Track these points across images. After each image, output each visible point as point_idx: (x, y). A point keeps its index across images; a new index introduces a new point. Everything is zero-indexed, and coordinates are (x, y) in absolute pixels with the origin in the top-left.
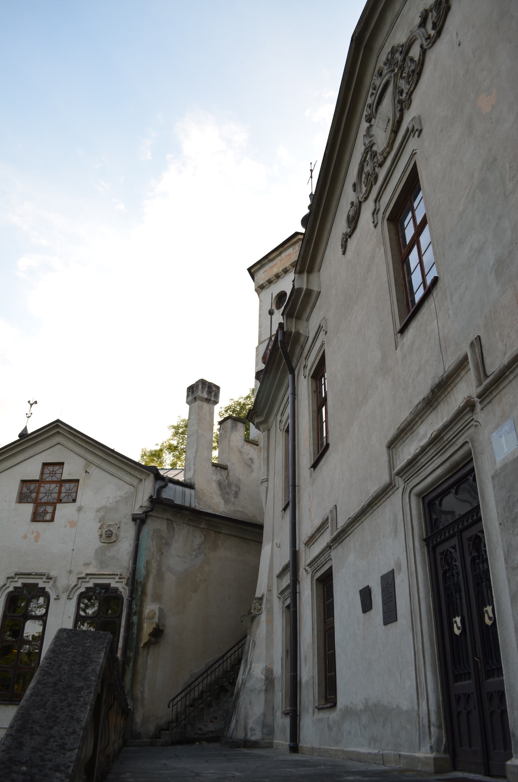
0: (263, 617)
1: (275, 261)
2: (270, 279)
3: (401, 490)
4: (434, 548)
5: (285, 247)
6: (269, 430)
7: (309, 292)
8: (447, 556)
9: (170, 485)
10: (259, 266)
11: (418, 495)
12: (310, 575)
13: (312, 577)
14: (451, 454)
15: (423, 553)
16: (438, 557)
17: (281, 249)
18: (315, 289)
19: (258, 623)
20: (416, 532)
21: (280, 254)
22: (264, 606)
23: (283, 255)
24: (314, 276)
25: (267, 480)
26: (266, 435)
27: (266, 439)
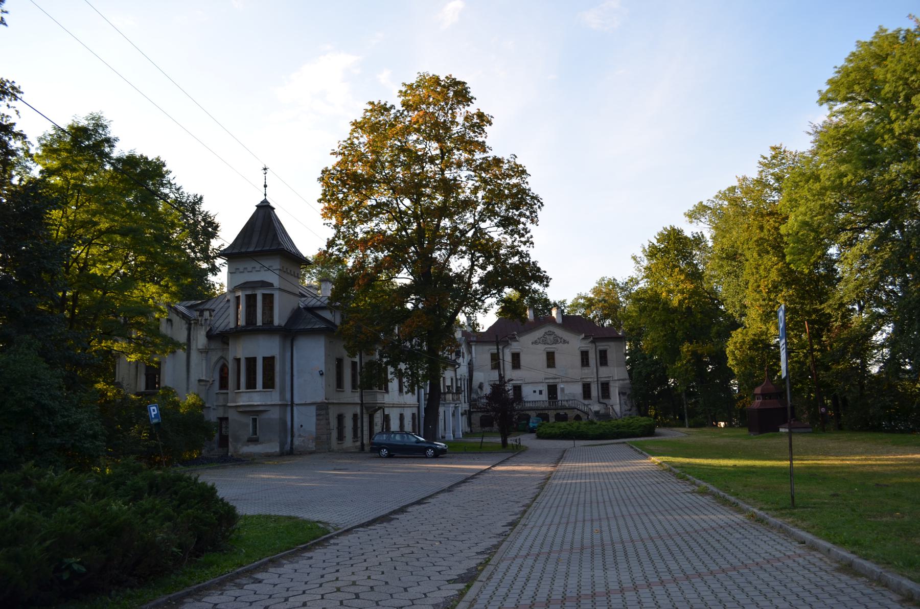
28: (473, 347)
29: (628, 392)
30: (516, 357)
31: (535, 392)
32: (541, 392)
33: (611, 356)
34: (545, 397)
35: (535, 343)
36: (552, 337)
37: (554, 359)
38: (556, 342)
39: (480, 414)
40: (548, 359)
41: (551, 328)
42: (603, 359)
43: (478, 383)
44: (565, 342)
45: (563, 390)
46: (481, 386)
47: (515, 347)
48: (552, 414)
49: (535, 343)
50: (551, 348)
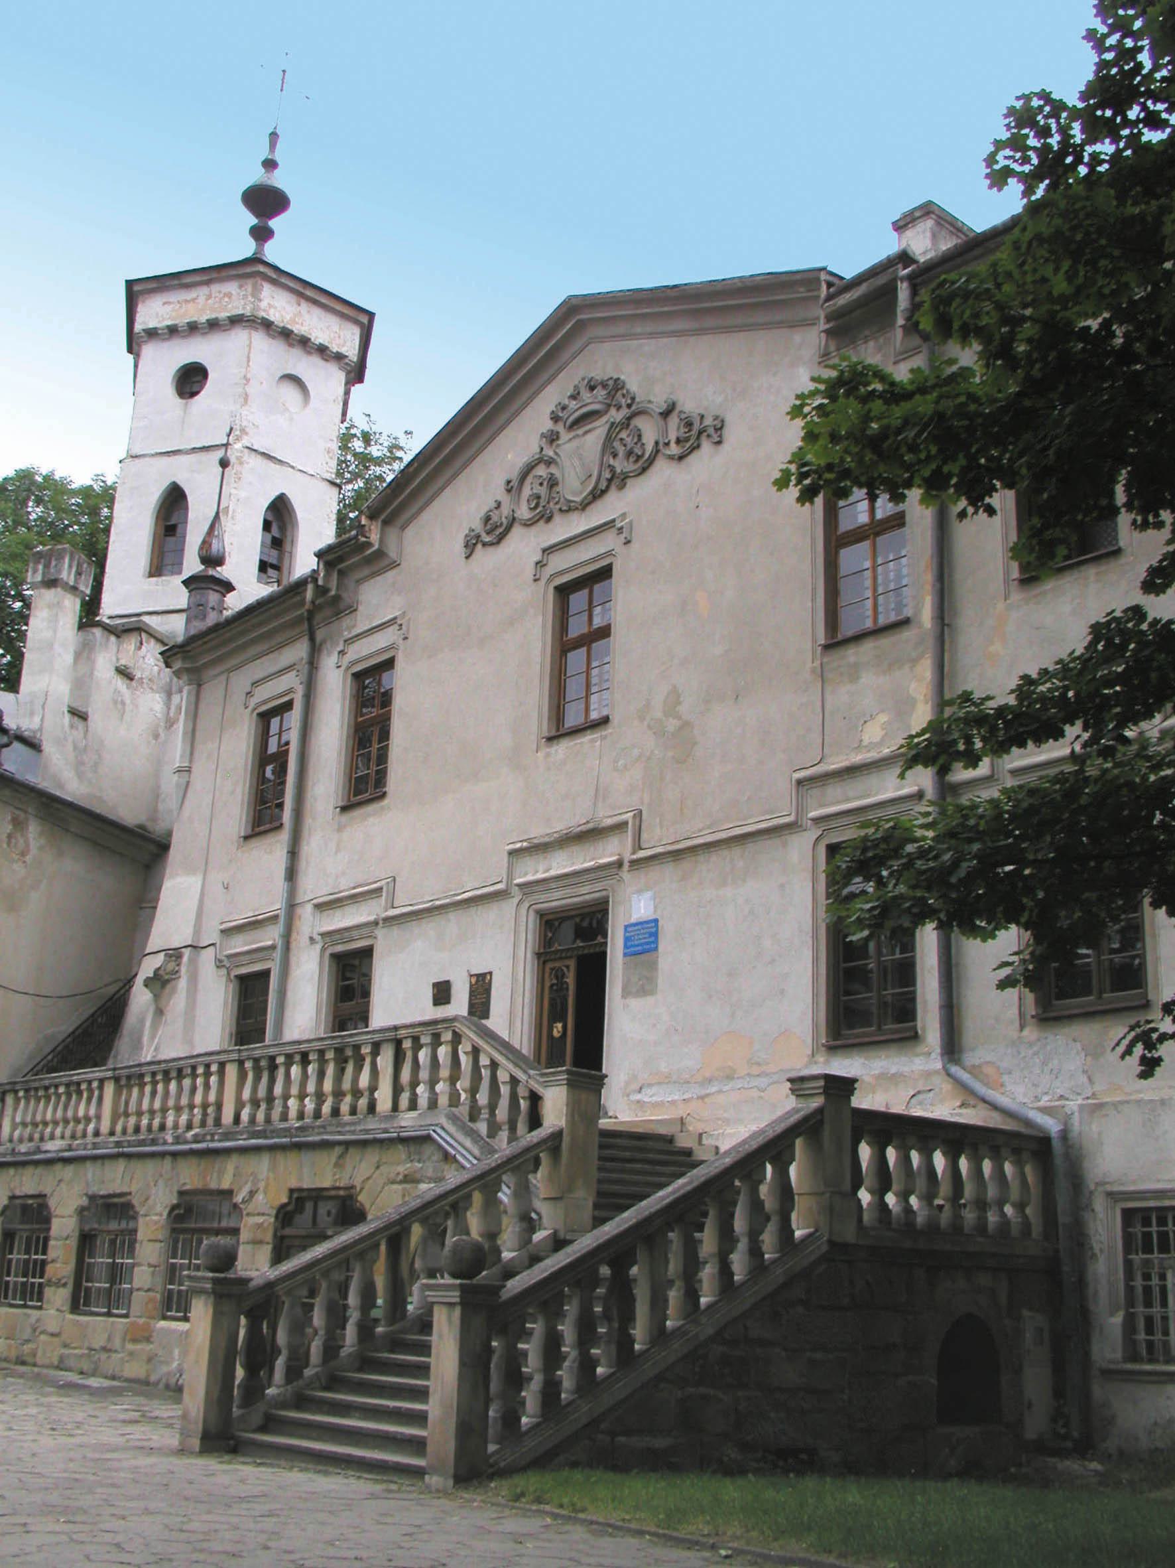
0: (182, 984)
1: (192, 294)
2: (176, 325)
3: (516, 901)
4: (544, 963)
5: (224, 274)
6: (199, 685)
7: (380, 554)
8: (560, 975)
9: (17, 745)
10: (154, 285)
11: (537, 912)
12: (318, 947)
13: (323, 949)
14: (585, 893)
15: (533, 965)
16: (547, 970)
17: (214, 275)
18: (392, 554)
19: (174, 990)
20: (530, 945)
21: (208, 283)
22: (183, 969)
23: (215, 288)
24: (392, 533)
25: (189, 770)
26: (194, 692)
27: (193, 699)
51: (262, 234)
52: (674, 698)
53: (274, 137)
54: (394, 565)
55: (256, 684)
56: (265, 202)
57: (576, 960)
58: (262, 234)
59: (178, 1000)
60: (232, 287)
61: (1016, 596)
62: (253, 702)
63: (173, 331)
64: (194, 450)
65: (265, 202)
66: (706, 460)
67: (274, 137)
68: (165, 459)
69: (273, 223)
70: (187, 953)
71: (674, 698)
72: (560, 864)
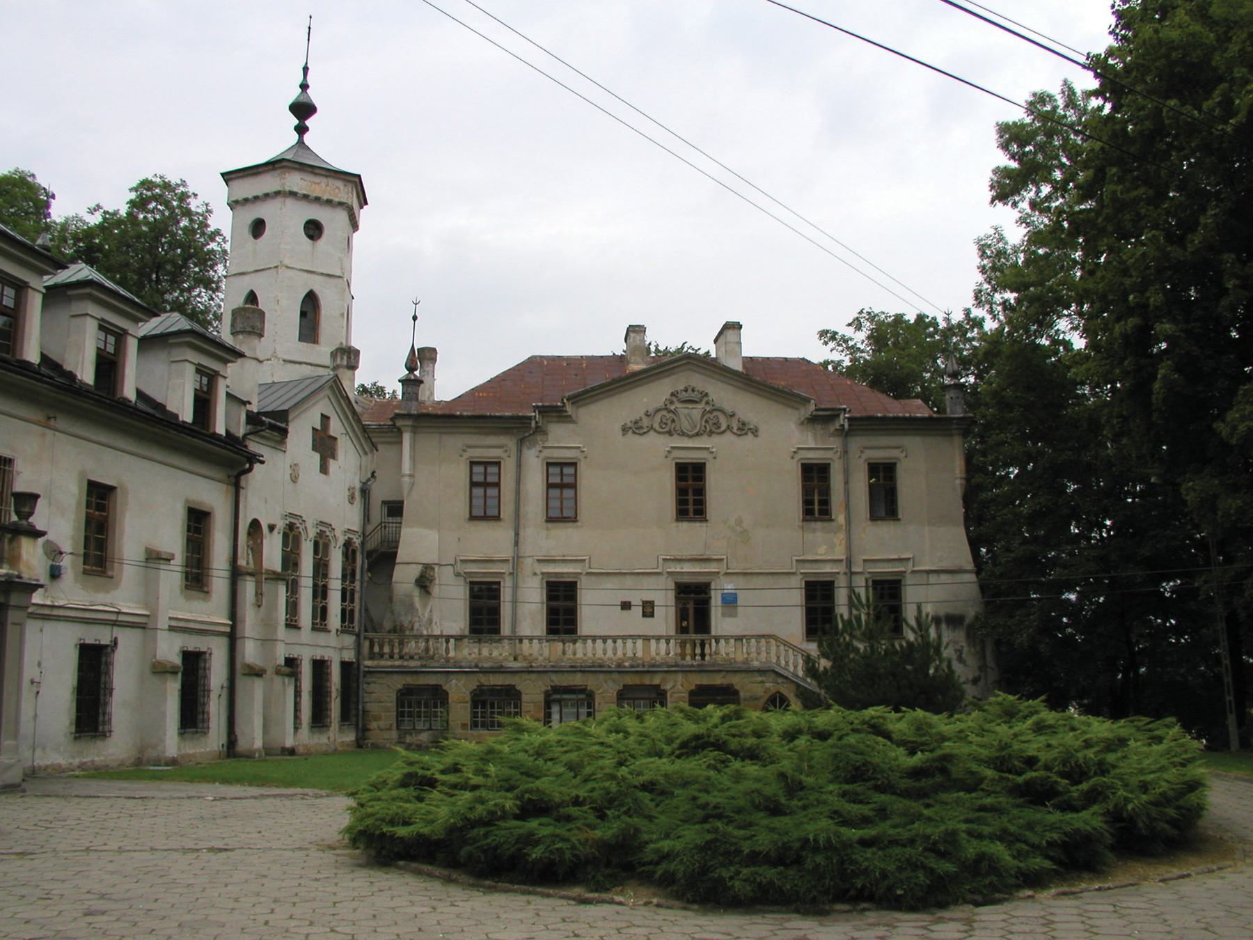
1: (317, 179)
14: (701, 579)
21: (326, 176)
23: (331, 181)
28: (407, 438)
29: (971, 613)
30: (563, 480)
31: (626, 606)
32: (648, 609)
33: (909, 487)
34: (664, 620)
35: (634, 428)
36: (696, 411)
37: (700, 492)
38: (712, 429)
39: (399, 682)
40: (681, 492)
41: (699, 381)
42: (884, 498)
43: (415, 572)
44: (744, 429)
45: (730, 602)
46: (424, 583)
47: (561, 439)
48: (678, 688)
49: (634, 428)
50: (692, 449)
51: (301, 130)
52: (739, 521)
53: (306, 70)
54: (574, 422)
55: (469, 447)
56: (302, 110)
57: (694, 604)
58: (301, 130)
59: (435, 590)
60: (340, 184)
61: (869, 523)
62: (466, 455)
63: (306, 197)
64: (322, 274)
65: (302, 110)
66: (749, 440)
67: (306, 70)
68: (305, 275)
69: (308, 123)
70: (436, 568)
71: (739, 521)
72: (687, 568)
